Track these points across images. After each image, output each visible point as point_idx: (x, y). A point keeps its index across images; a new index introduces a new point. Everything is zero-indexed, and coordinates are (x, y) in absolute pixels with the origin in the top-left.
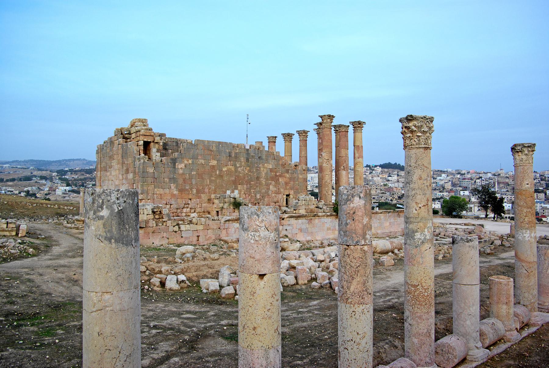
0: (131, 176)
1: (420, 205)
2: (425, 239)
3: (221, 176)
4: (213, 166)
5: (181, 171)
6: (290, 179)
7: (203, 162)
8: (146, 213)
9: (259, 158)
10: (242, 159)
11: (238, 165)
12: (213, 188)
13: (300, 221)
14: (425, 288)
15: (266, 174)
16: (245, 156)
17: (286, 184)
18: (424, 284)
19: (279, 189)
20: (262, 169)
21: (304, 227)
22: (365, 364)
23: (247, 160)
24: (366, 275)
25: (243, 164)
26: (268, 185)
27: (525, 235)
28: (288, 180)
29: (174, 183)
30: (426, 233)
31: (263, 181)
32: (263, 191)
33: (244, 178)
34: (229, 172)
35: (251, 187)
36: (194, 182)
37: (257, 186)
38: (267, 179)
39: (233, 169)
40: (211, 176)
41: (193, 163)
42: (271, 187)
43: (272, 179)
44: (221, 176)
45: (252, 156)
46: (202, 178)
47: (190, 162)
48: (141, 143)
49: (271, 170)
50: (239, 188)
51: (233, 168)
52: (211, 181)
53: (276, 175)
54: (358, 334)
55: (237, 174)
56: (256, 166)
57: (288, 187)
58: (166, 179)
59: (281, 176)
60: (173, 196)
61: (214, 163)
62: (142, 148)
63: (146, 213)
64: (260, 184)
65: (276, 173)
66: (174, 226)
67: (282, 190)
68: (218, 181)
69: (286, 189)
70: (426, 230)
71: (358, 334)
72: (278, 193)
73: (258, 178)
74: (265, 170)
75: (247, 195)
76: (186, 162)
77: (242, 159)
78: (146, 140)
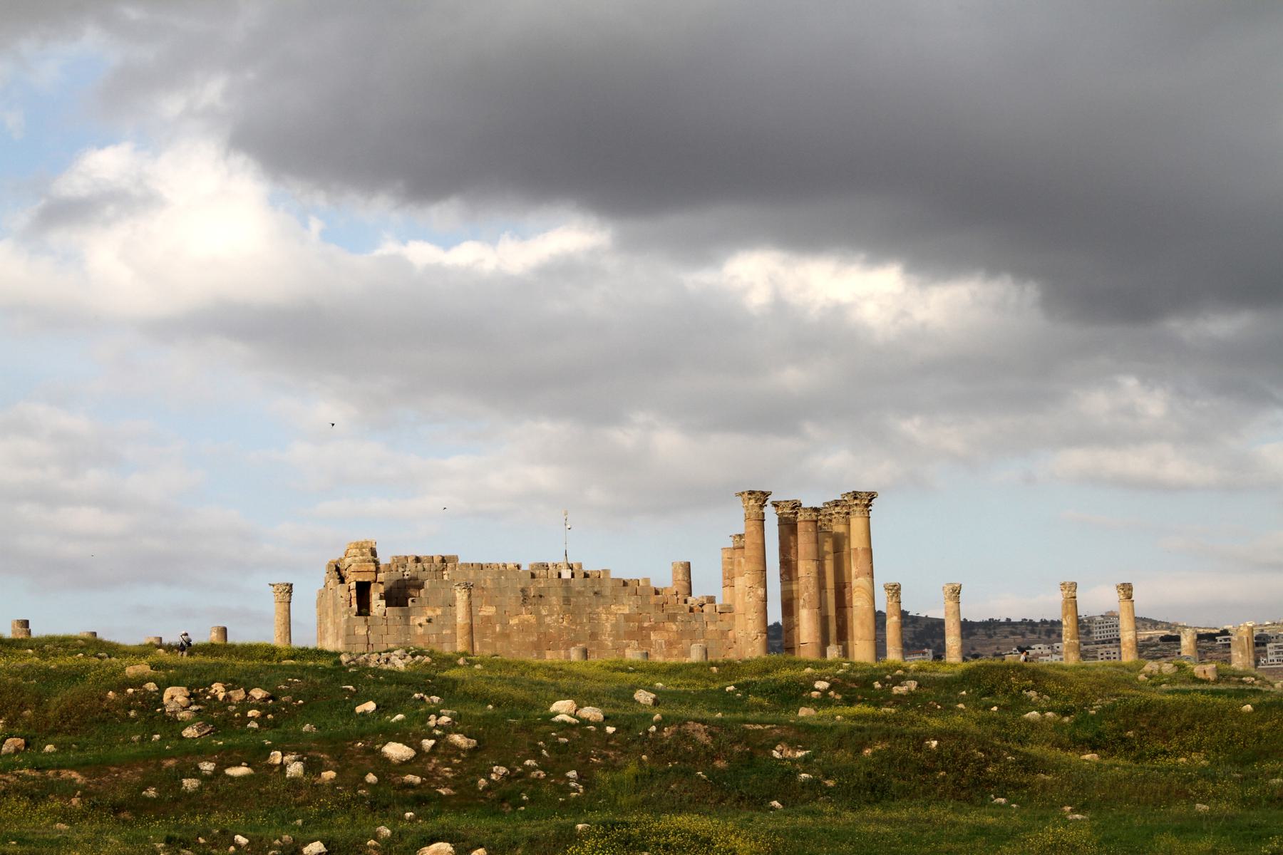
4: (488, 618)
5: (420, 631)
6: (681, 634)
10: (554, 600)
11: (544, 613)
15: (615, 626)
16: (561, 593)
23: (567, 601)
25: (556, 608)
28: (673, 636)
33: (560, 636)
34: (524, 628)
38: (617, 636)
41: (444, 614)
43: (631, 635)
44: (505, 635)
45: (579, 592)
47: (439, 612)
49: (628, 618)
51: (532, 619)
53: (641, 628)
55: (542, 630)
56: (589, 610)
57: (675, 652)
59: (653, 628)
62: (354, 593)
65: (641, 622)
68: (498, 645)
73: (594, 636)
74: (612, 617)
76: (430, 613)
77: (554, 600)
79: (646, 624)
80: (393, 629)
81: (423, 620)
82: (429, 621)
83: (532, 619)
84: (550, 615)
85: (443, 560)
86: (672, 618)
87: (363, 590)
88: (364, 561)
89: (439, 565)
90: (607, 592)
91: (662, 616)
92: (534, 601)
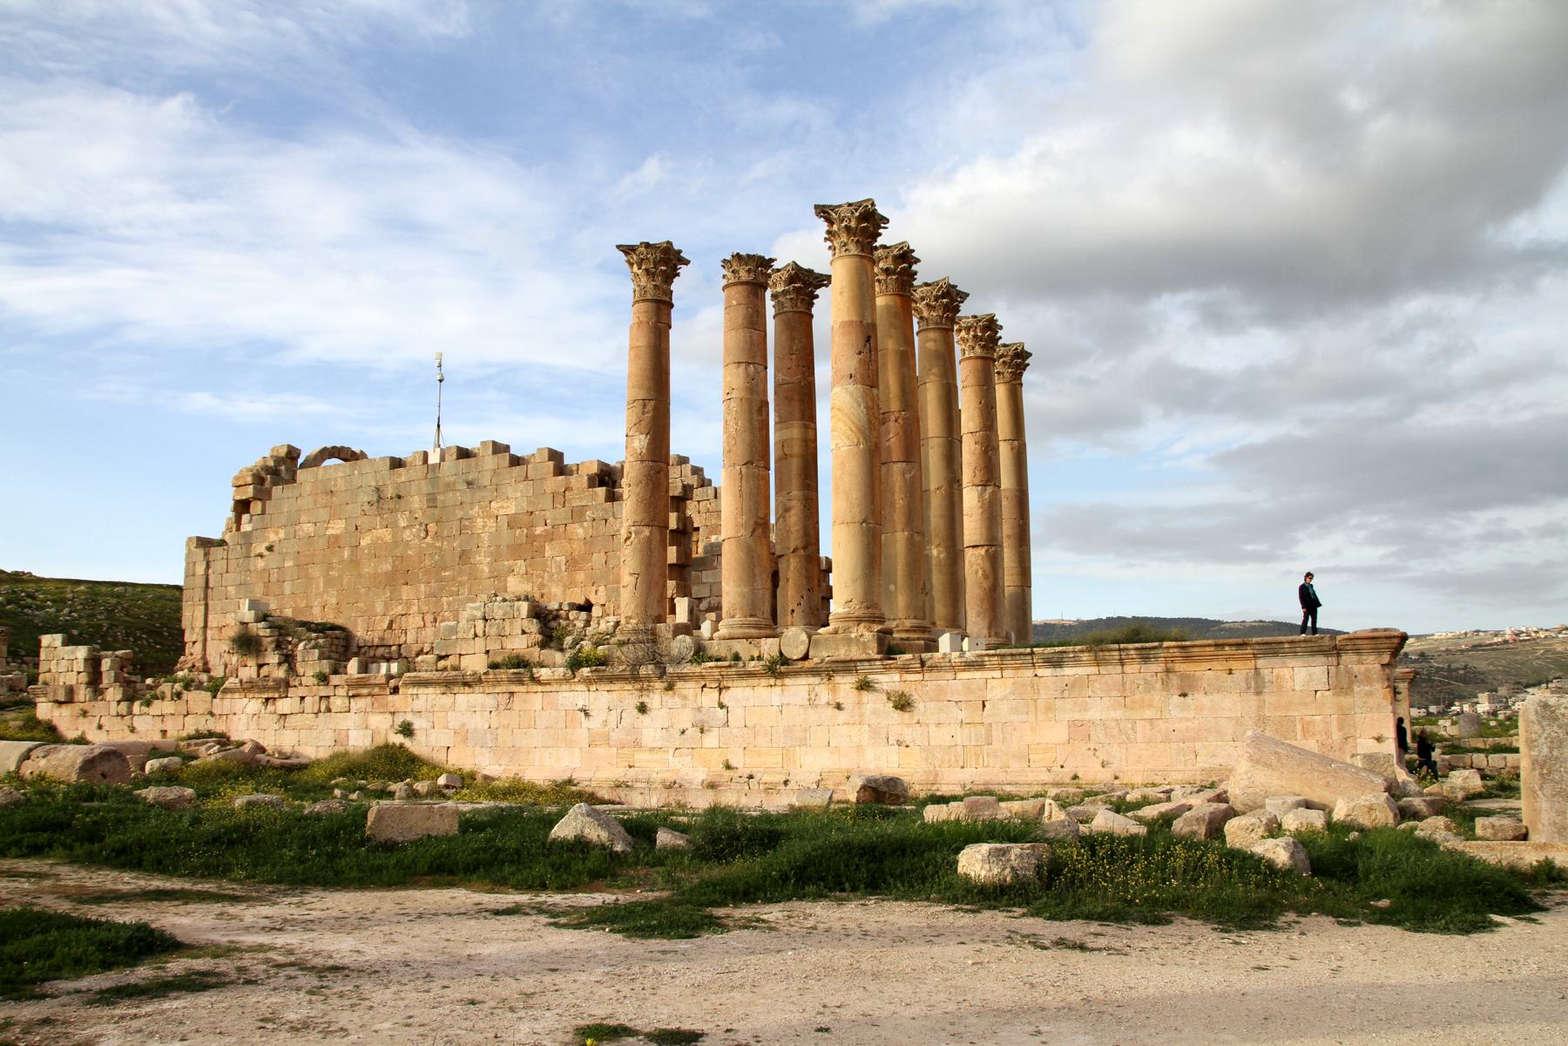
3: (355, 562)
4: (336, 537)
6: (589, 541)
7: (308, 528)
9: (469, 484)
11: (402, 523)
12: (334, 601)
13: (464, 698)
16: (425, 487)
17: (573, 563)
19: (542, 586)
20: (480, 522)
21: (478, 722)
23: (432, 501)
26: (499, 576)
31: (483, 561)
34: (376, 552)
35: (443, 588)
36: (287, 588)
37: (462, 584)
39: (389, 538)
40: (330, 566)
43: (516, 551)
44: (355, 562)
45: (448, 485)
46: (308, 578)
47: (282, 535)
49: (513, 522)
51: (385, 534)
52: (329, 583)
53: (531, 538)
55: (398, 552)
56: (460, 513)
57: (581, 576)
59: (550, 537)
61: (337, 528)
64: (474, 576)
65: (532, 526)
69: (572, 584)
73: (464, 556)
75: (429, 618)
76: (272, 537)
79: (539, 530)
80: (233, 563)
81: (262, 549)
82: (270, 549)
83: (385, 534)
86: (577, 515)
90: (486, 480)
91: (562, 514)
92: (391, 505)
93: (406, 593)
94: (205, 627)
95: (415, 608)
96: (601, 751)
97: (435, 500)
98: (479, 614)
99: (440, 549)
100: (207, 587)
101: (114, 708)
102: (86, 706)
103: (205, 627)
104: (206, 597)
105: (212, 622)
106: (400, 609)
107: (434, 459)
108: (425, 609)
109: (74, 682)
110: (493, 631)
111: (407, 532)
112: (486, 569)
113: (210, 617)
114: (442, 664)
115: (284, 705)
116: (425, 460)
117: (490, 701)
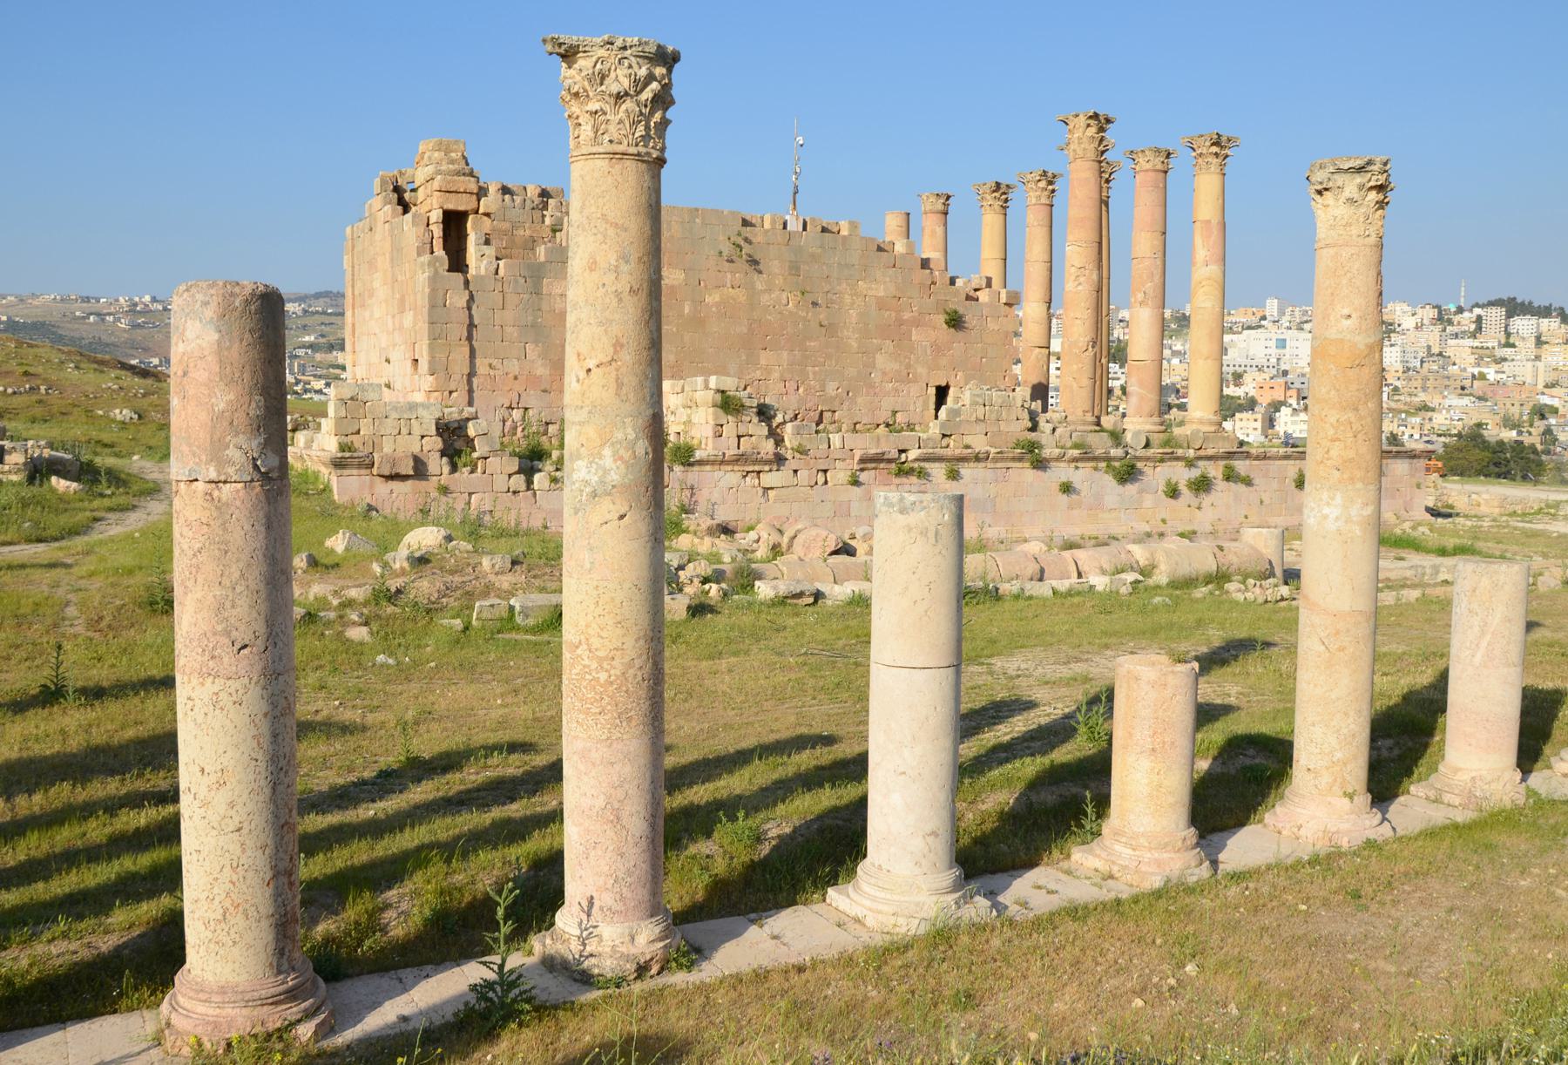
0: (408, 319)
1: (591, 364)
2: (602, 482)
8: (417, 431)
11: (759, 286)
14: (601, 654)
18: (596, 642)
19: (908, 366)
22: (227, 870)
23: (795, 269)
24: (226, 582)
25: (779, 281)
27: (1326, 510)
29: (536, 342)
30: (608, 462)
32: (852, 372)
39: (742, 299)
42: (880, 360)
45: (813, 256)
48: (436, 216)
49: (881, 305)
50: (763, 362)
51: (740, 295)
53: (900, 323)
54: (203, 770)
57: (944, 361)
58: (508, 330)
59: (917, 323)
60: (533, 380)
62: (437, 231)
63: (417, 431)
66: (510, 476)
67: (921, 370)
70: (607, 452)
71: (203, 770)
72: (906, 378)
73: (829, 329)
75: (791, 386)
78: (450, 206)
80: (512, 299)
84: (769, 291)
85: (545, 194)
87: (454, 223)
88: (458, 173)
89: (537, 200)
93: (765, 358)
94: (471, 375)
95: (776, 375)
96: (1076, 512)
97: (798, 269)
98: (981, 401)
99: (805, 319)
100: (471, 326)
101: (501, 482)
102: (445, 479)
103: (471, 375)
104: (470, 338)
105: (482, 367)
106: (758, 374)
107: (794, 225)
108: (787, 376)
109: (416, 449)
110: (994, 416)
111: (766, 297)
112: (855, 345)
113: (478, 361)
114: (944, 442)
115: (769, 479)
116: (785, 227)
117: (989, 474)
